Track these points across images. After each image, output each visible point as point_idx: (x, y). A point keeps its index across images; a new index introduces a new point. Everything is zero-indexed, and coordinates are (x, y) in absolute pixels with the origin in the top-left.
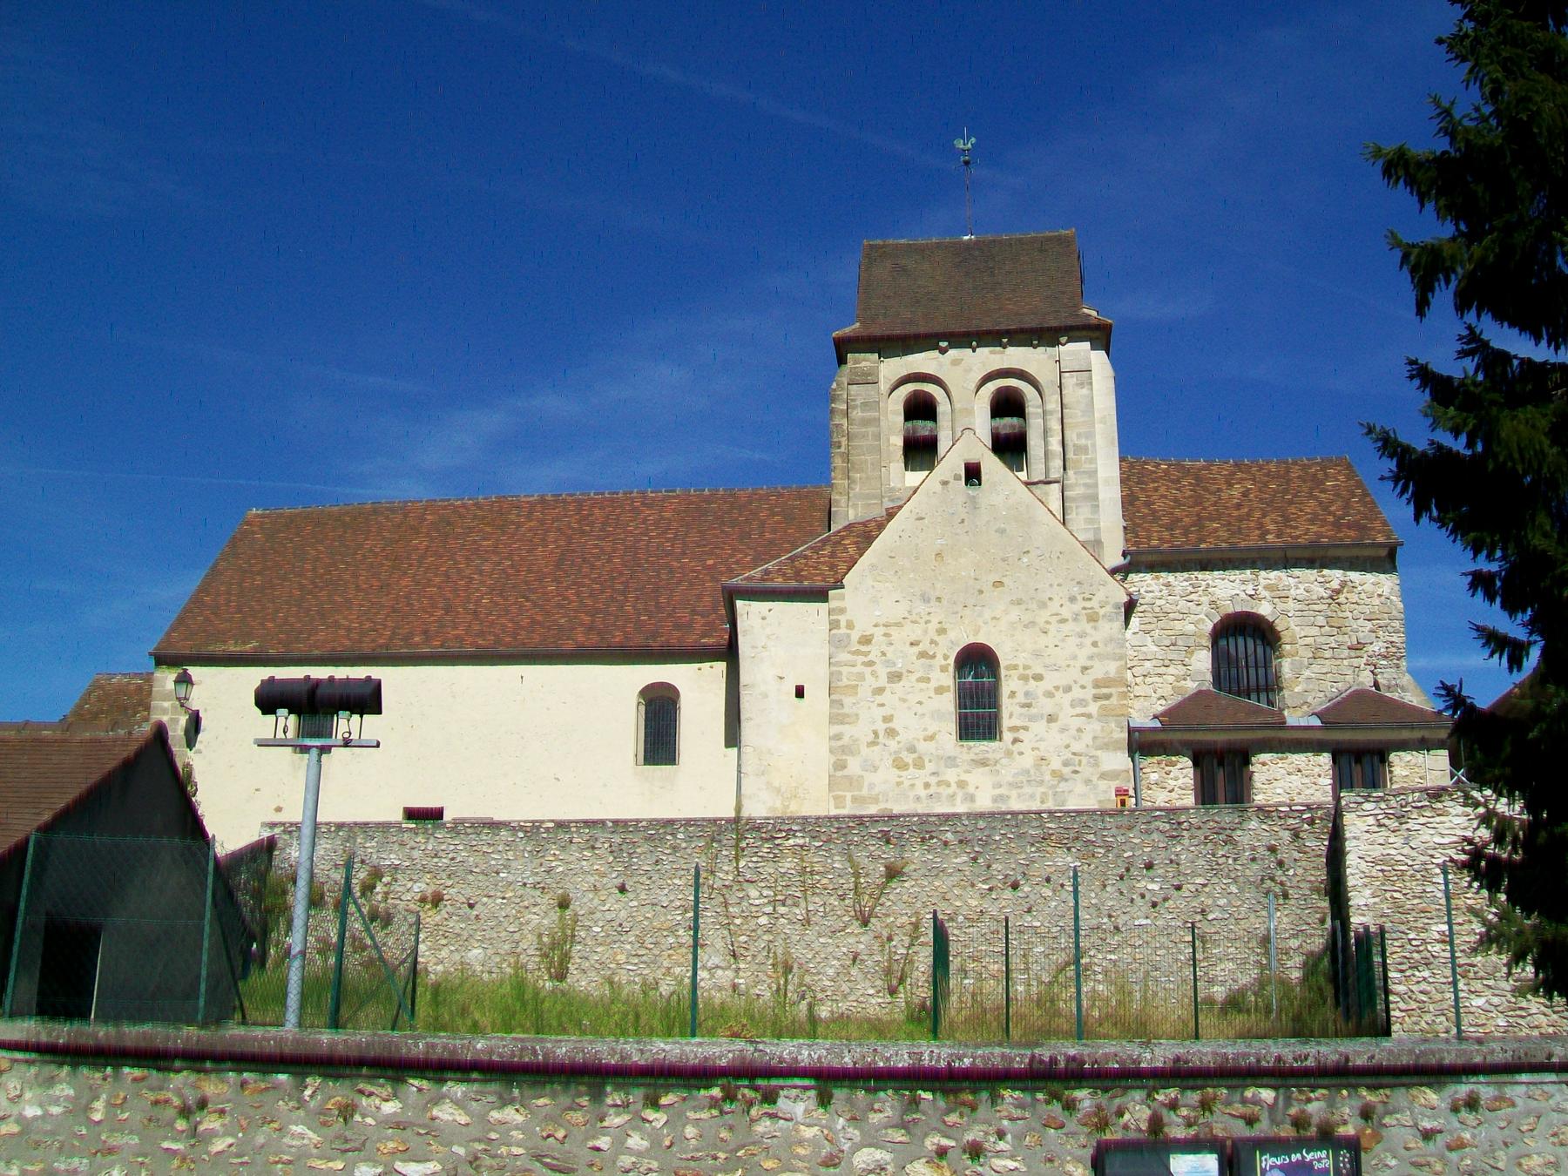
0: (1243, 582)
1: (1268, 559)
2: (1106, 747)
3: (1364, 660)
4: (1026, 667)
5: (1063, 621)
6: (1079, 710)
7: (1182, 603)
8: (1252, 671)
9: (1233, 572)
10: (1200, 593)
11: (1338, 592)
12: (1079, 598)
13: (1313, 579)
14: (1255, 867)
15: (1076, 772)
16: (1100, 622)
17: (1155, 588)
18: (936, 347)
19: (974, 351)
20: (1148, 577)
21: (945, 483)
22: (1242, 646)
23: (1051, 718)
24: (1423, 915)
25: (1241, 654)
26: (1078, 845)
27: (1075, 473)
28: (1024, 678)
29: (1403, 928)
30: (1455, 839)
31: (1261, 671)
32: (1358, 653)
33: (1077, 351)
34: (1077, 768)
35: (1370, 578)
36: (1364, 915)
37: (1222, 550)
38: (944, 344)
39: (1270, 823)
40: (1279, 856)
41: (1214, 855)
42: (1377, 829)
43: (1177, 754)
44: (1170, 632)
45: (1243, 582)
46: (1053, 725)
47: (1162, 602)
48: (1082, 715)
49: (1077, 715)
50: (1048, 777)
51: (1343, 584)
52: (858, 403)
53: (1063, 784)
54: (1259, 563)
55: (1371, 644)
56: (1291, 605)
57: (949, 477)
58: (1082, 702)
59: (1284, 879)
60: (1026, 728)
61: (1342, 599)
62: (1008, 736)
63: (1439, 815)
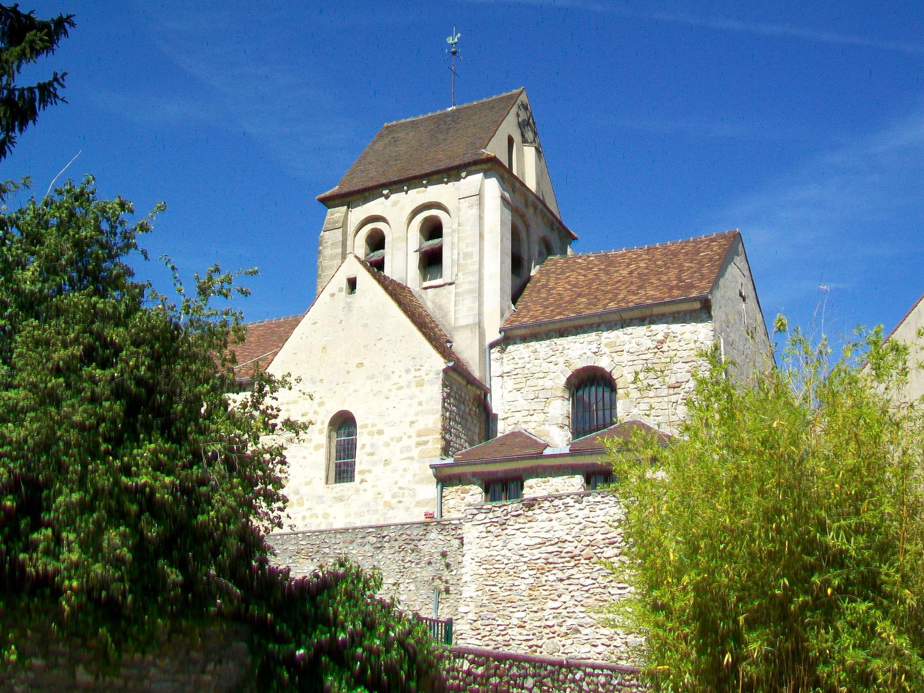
0: (590, 343)
1: (610, 322)
2: (421, 481)
3: (681, 396)
4: (374, 425)
5: (401, 388)
6: (406, 455)
7: (545, 365)
8: (600, 413)
9: (582, 336)
10: (558, 355)
11: (662, 342)
12: (413, 369)
13: (642, 334)
14: (430, 568)
15: (400, 502)
16: (425, 386)
17: (526, 355)
18: (382, 195)
19: (406, 193)
20: (521, 347)
21: (333, 295)
22: (592, 394)
23: (387, 462)
24: (510, 604)
25: (593, 400)
26: (318, 556)
27: (463, 274)
28: (371, 434)
29: (495, 615)
30: (539, 540)
31: (607, 412)
32: (676, 390)
33: (473, 182)
34: (401, 499)
35: (690, 327)
36: (468, 606)
37: (571, 319)
38: (385, 192)
39: (445, 534)
40: (447, 561)
41: (403, 561)
42: (484, 535)
43: (470, 483)
44: (534, 388)
45: (590, 343)
46: (387, 467)
47: (531, 365)
48: (408, 458)
49: (404, 459)
50: (381, 507)
51: (667, 336)
52: (329, 244)
53: (391, 512)
54: (602, 327)
55: (687, 382)
56: (626, 357)
57: (335, 290)
58: (408, 449)
59: (448, 578)
60: (369, 471)
61: (665, 348)
62: (358, 477)
63: (530, 521)
